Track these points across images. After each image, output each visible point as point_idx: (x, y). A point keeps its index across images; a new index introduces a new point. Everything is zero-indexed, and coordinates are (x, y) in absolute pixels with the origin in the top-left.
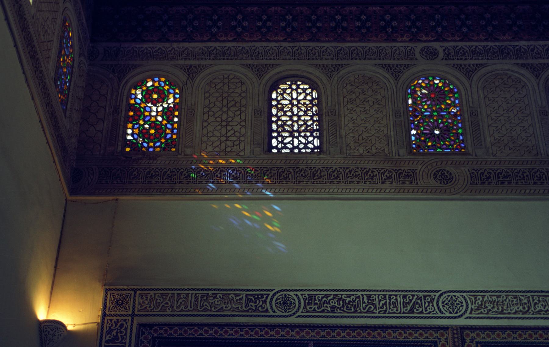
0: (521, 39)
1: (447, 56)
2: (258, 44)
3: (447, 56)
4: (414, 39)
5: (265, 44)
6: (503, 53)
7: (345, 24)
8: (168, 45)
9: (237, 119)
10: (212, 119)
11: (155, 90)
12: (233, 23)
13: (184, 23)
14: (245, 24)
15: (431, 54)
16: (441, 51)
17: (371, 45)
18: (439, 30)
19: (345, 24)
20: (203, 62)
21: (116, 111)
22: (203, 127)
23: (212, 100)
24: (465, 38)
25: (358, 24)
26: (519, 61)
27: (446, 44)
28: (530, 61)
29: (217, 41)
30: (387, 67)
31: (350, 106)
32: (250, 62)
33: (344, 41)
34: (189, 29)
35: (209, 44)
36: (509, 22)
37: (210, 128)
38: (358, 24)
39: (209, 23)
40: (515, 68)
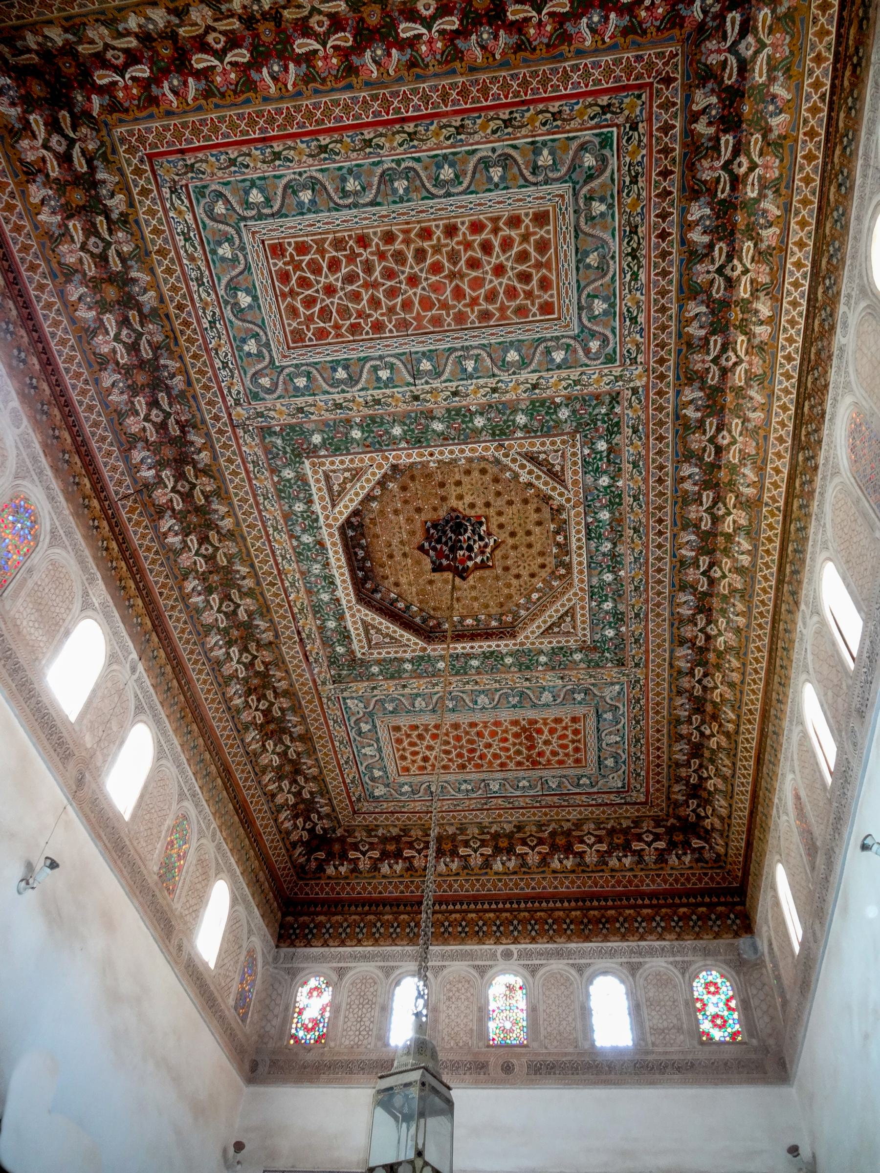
0: (572, 942)
1: (520, 957)
2: (389, 948)
3: (520, 957)
4: (498, 942)
5: (394, 948)
6: (559, 954)
7: (450, 929)
8: (327, 949)
9: (368, 1015)
10: (351, 1015)
11: (316, 988)
12: (374, 930)
13: (340, 930)
14: (382, 930)
15: (508, 955)
16: (515, 952)
17: (468, 947)
18: (516, 933)
19: (450, 929)
20: (349, 965)
21: (287, 1008)
22: (345, 1022)
23: (353, 998)
24: (533, 940)
25: (460, 929)
26: (571, 962)
27: (519, 946)
28: (577, 961)
29: (362, 945)
30: (476, 967)
31: (448, 1003)
32: (382, 964)
33: (449, 945)
34: (344, 935)
35: (356, 948)
36: (565, 926)
37: (349, 1024)
38: (460, 929)
39: (358, 930)
40: (567, 968)
